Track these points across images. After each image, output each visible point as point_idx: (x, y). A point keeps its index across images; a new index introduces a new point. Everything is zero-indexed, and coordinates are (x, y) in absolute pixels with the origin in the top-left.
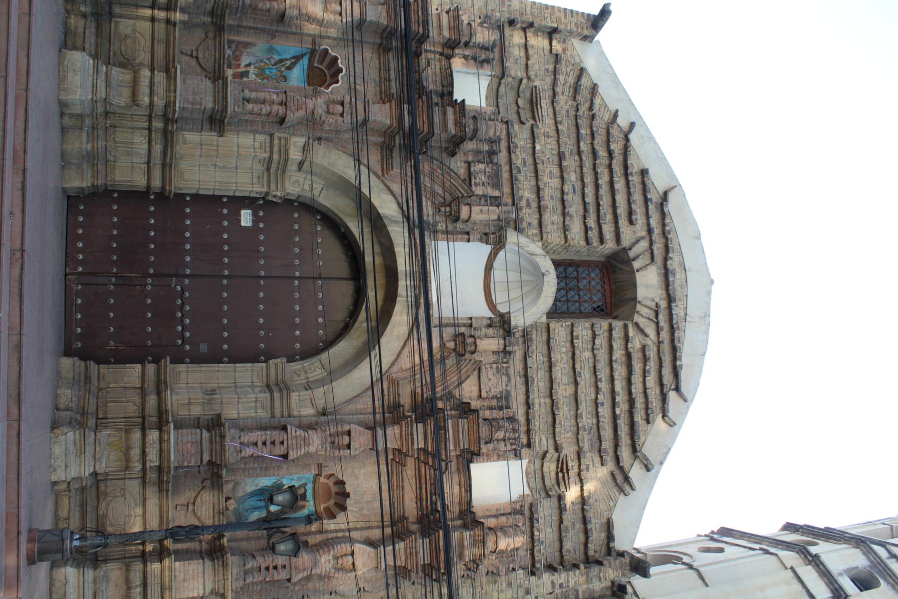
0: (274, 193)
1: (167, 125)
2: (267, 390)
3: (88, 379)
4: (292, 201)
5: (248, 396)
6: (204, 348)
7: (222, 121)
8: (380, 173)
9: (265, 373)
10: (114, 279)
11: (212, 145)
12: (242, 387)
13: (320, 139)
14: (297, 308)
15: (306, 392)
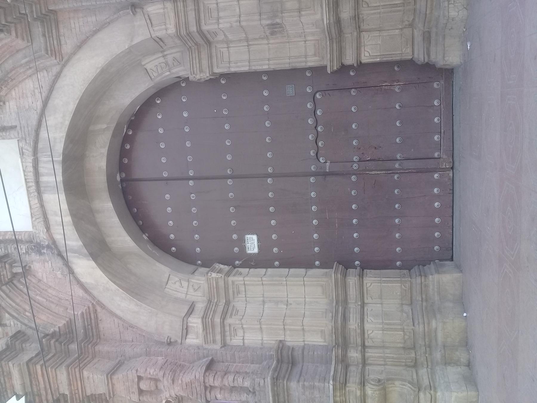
0: (220, 275)
1: (343, 353)
2: (208, 36)
3: (427, 37)
4: (203, 265)
5: (228, 25)
6: (290, 90)
7: (280, 361)
8: (99, 309)
9: (214, 60)
10: (397, 166)
11: (290, 330)
12: (240, 41)
13: (170, 344)
14: (188, 144)
15: (160, 34)
